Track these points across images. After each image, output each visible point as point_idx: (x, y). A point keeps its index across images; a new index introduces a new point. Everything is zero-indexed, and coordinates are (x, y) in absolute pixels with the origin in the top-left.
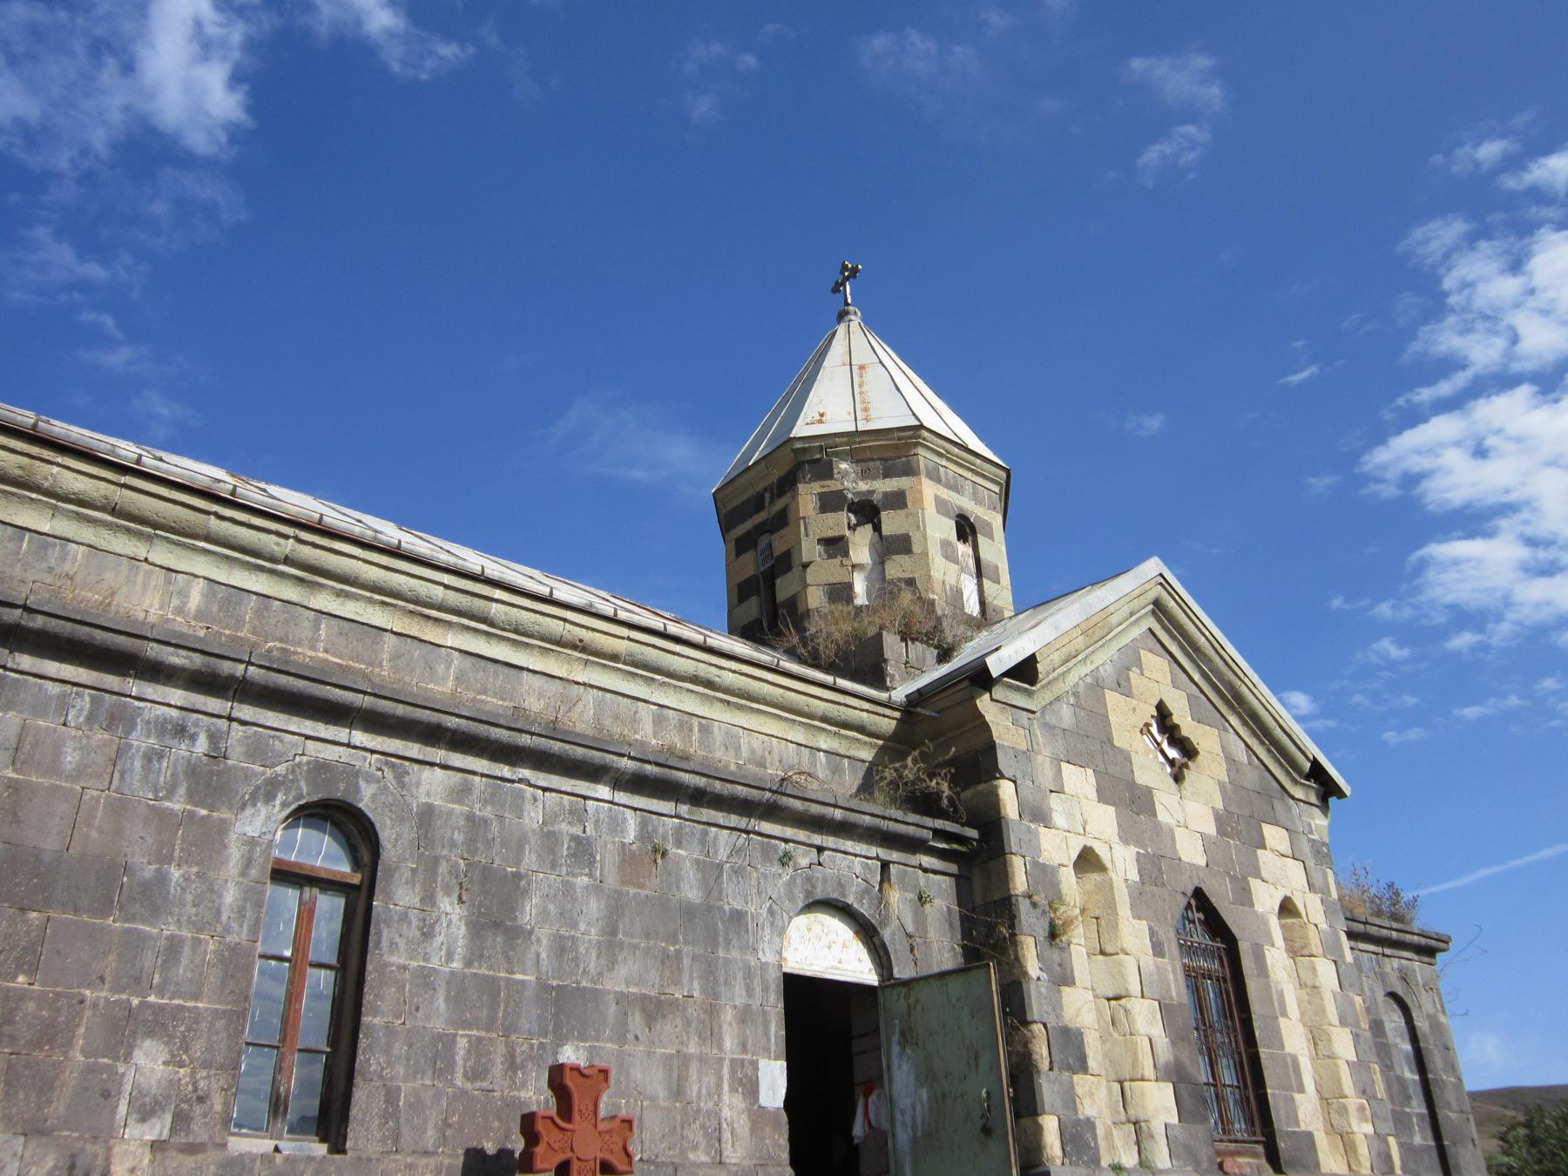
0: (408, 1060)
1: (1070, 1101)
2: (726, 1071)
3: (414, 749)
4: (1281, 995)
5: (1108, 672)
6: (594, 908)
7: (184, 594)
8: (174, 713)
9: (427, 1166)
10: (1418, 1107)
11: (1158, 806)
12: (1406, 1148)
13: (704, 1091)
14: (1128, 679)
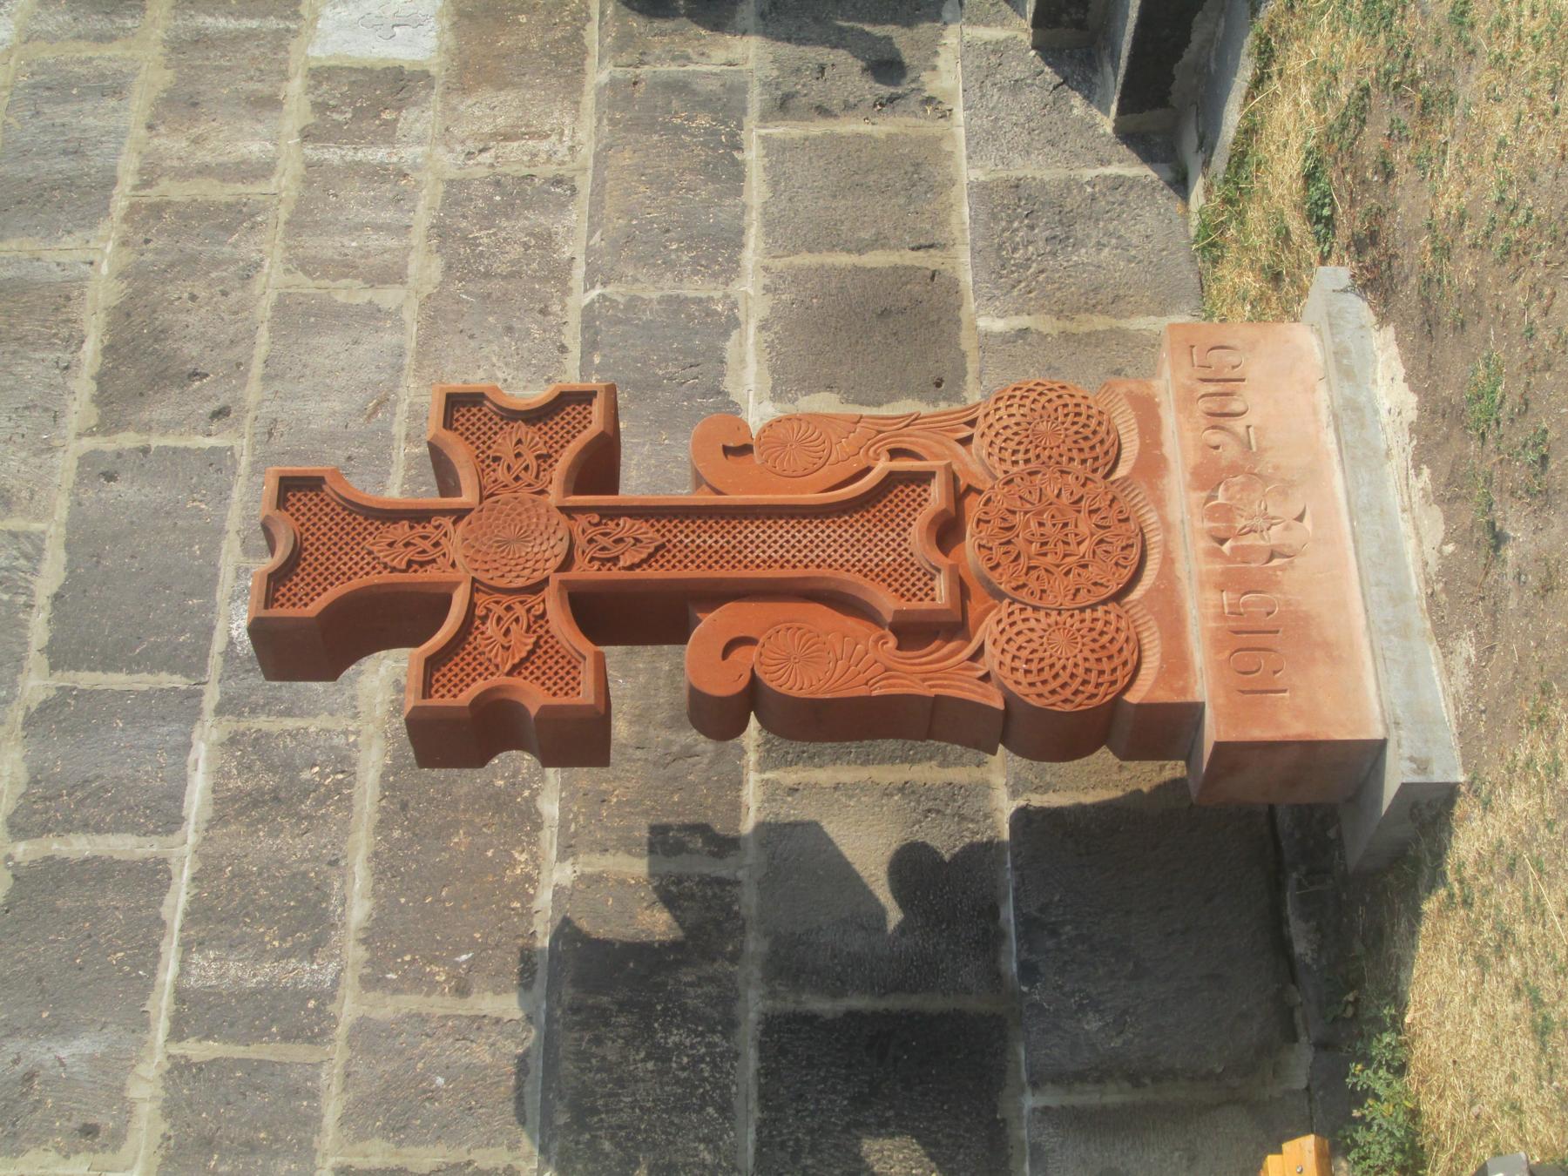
0: (252, 1147)
2: (333, 155)
9: (582, 1056)
13: (387, 216)
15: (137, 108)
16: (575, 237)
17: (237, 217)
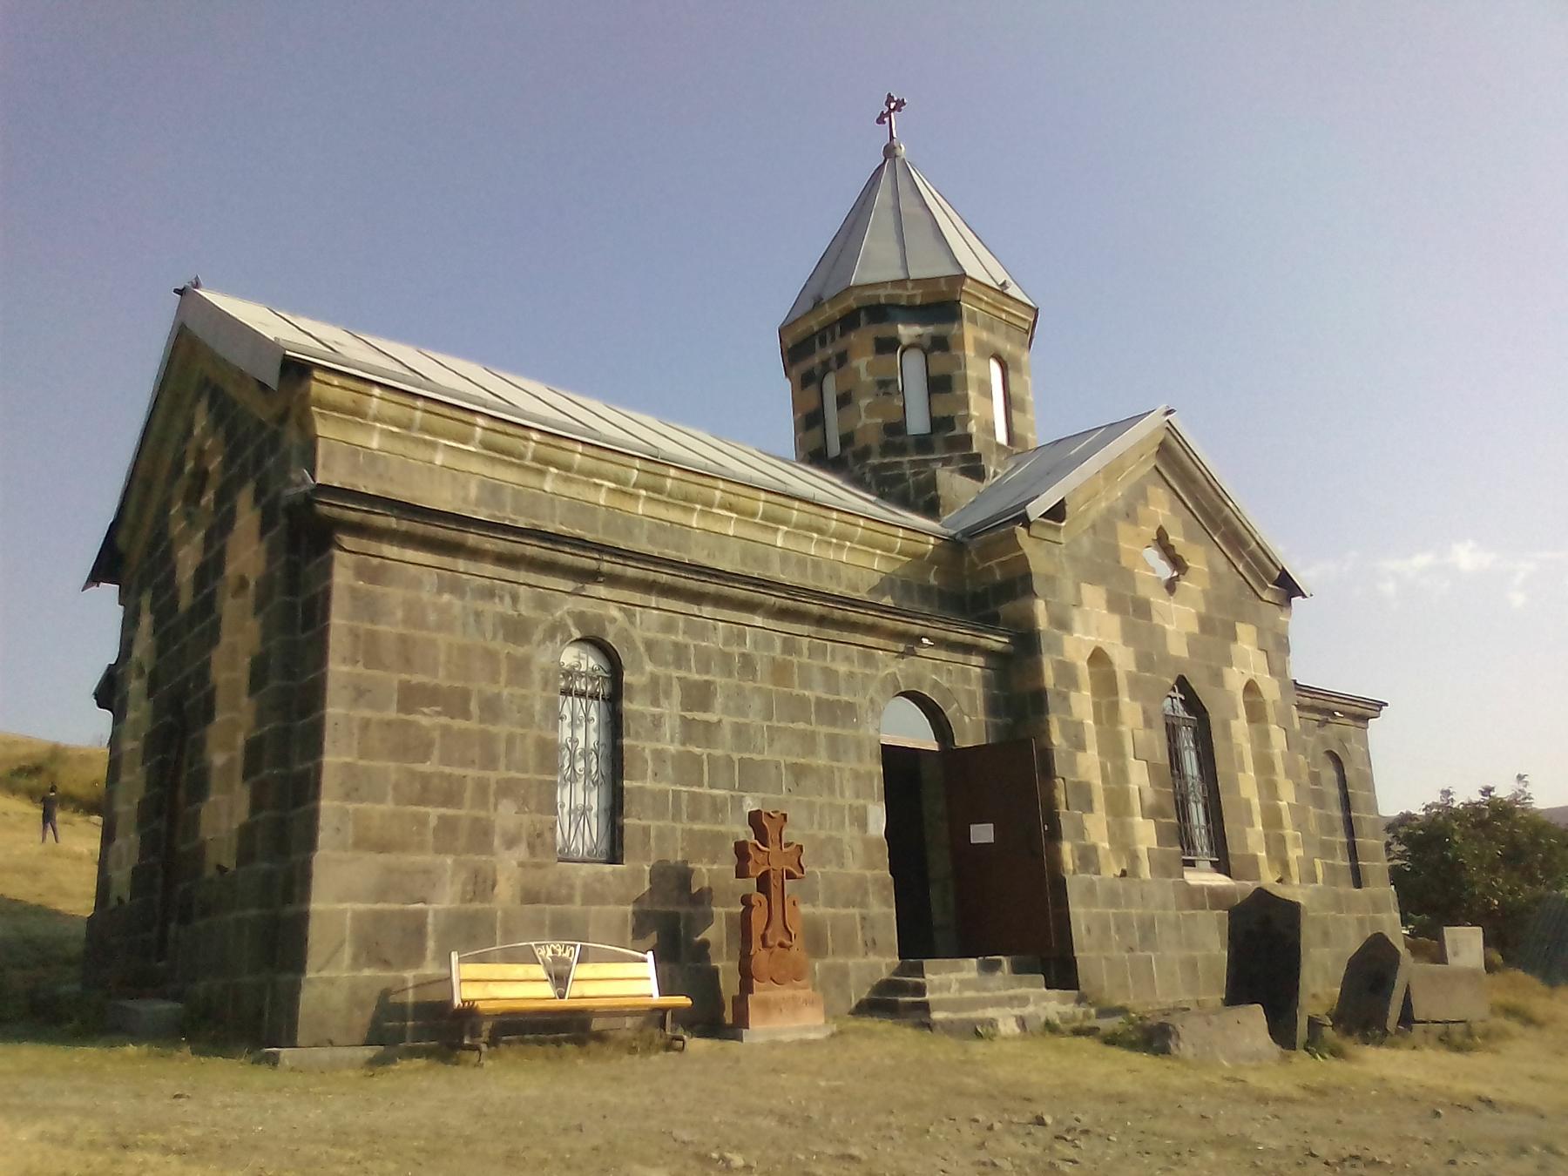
1: (1080, 831)
3: (637, 597)
4: (1241, 754)
5: (1121, 505)
6: (757, 703)
7: (465, 487)
8: (488, 582)
10: (1341, 838)
11: (1154, 613)
12: (1331, 870)
14: (1135, 510)
15: (855, 765)
16: (831, 869)
17: (832, 791)
